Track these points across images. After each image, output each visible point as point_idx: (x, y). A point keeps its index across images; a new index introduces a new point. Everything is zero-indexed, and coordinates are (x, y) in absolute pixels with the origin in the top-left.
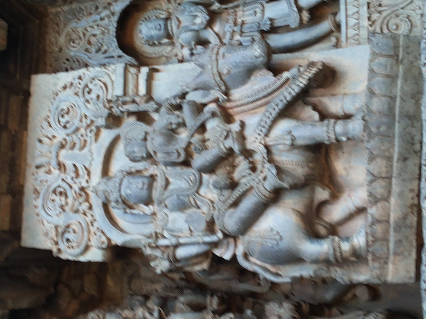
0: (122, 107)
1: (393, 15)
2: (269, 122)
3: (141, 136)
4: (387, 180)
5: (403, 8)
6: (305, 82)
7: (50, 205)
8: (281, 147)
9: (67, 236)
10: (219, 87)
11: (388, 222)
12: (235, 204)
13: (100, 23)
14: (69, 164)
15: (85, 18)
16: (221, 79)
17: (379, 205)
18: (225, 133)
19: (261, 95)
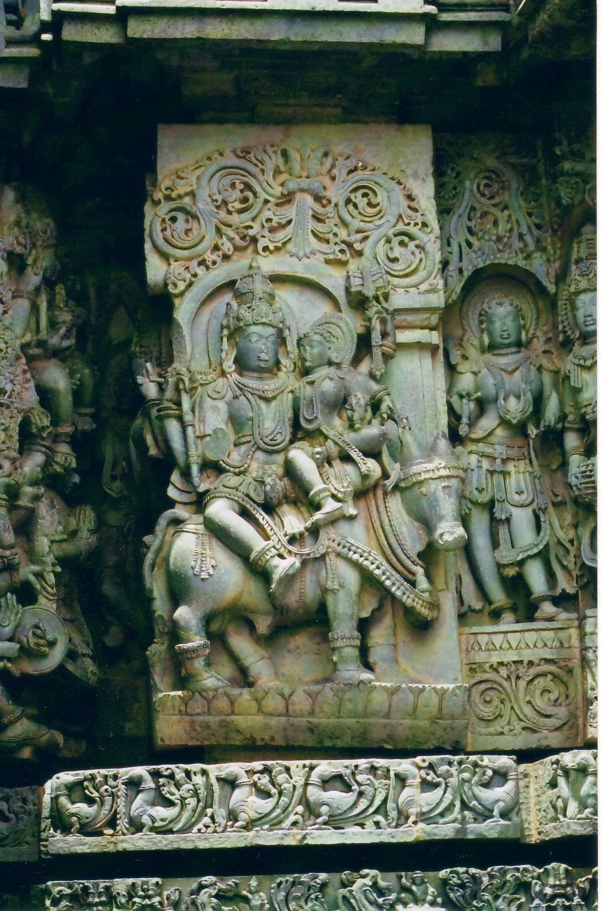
0: (378, 318)
1: (503, 696)
2: (356, 557)
3: (335, 357)
4: (284, 711)
5: (512, 708)
6: (409, 602)
7: (227, 181)
8: (323, 573)
9: (181, 217)
10: (404, 479)
11: (233, 713)
12: (244, 513)
13: (515, 233)
14: (290, 212)
15: (523, 204)
16: (414, 484)
17: (254, 704)
18: (340, 495)
19: (393, 540)
